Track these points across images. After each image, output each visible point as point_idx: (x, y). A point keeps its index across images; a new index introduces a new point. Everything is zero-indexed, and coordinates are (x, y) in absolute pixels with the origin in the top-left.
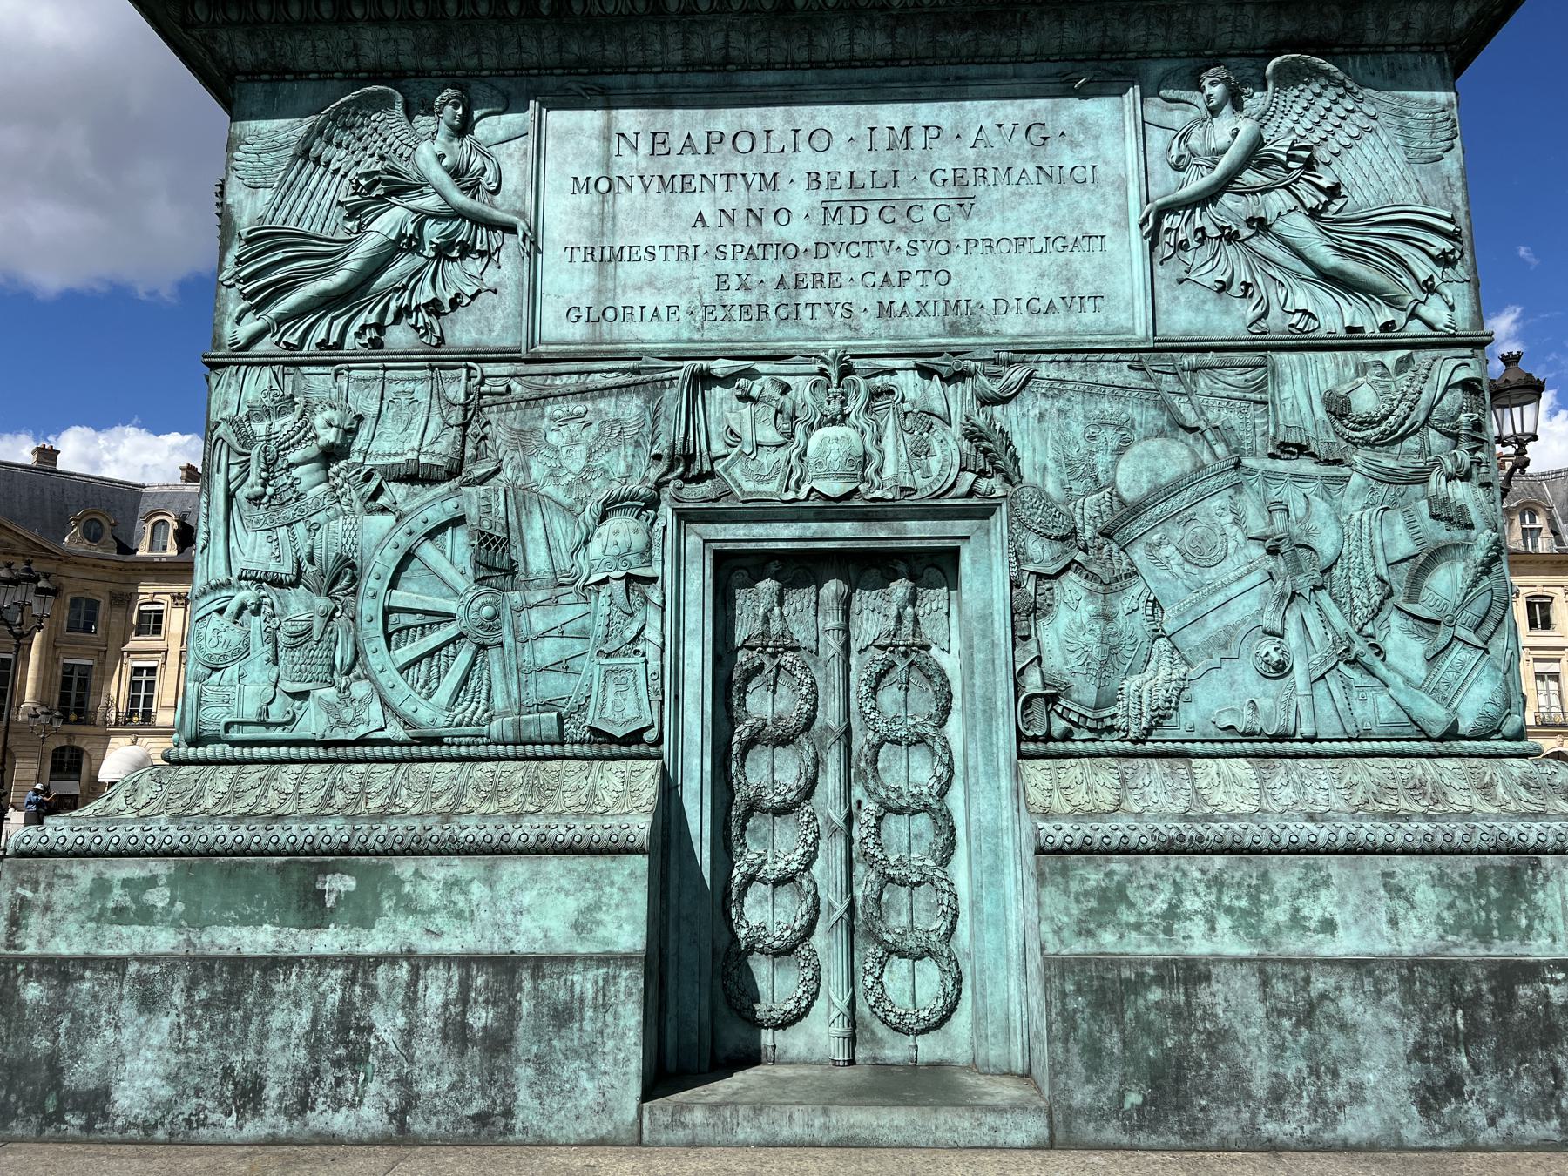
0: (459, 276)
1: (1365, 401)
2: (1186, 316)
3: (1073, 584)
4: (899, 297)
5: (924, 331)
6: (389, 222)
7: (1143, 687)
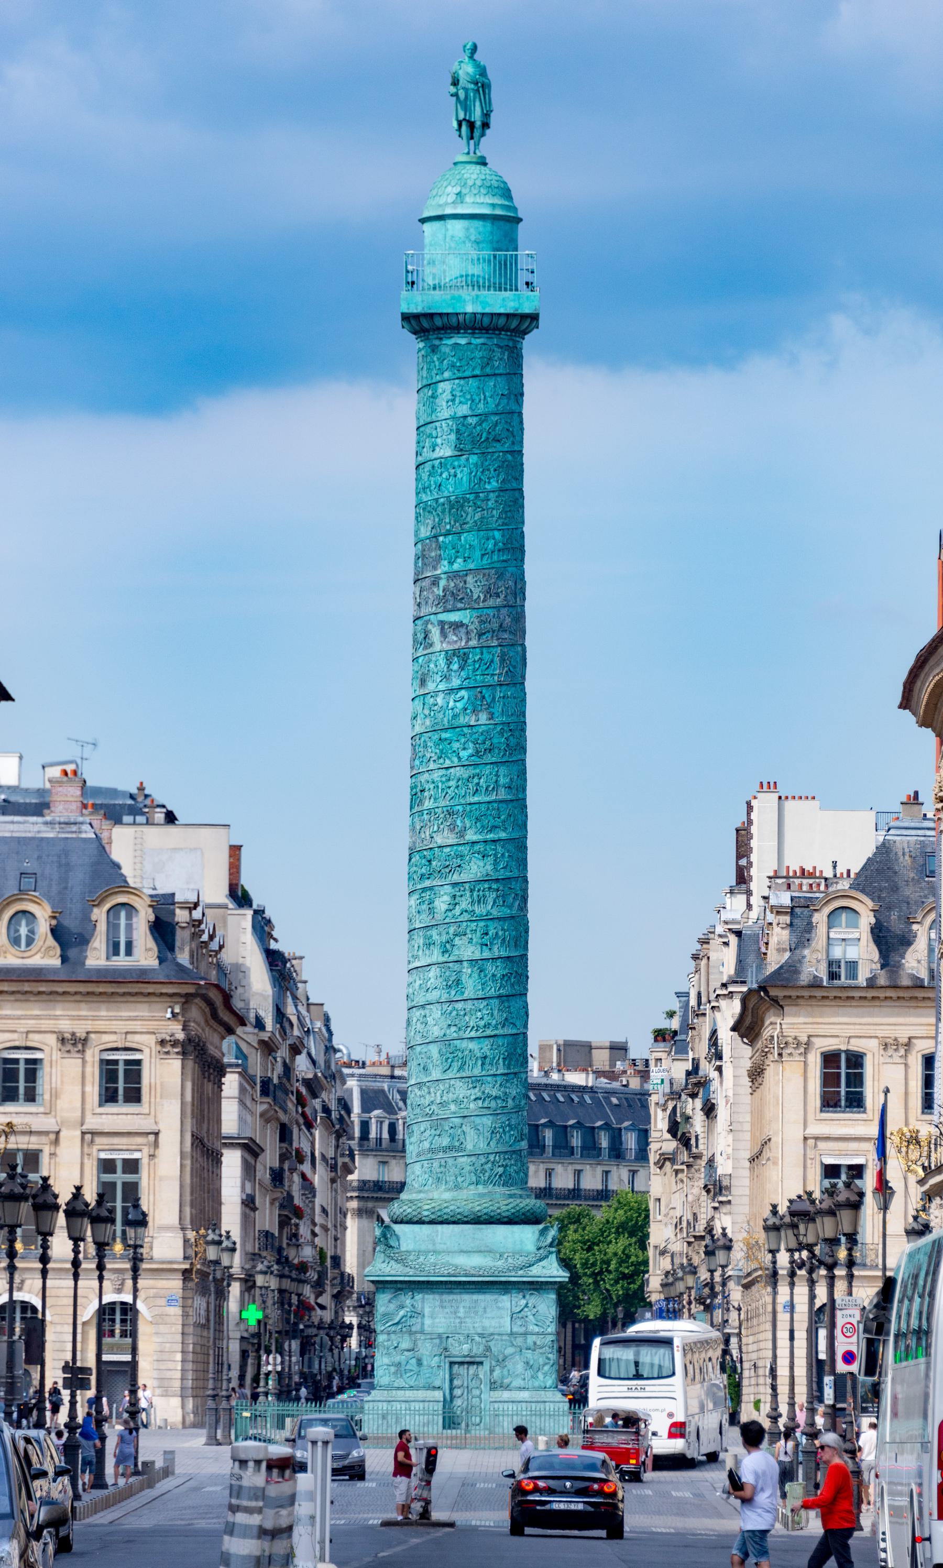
0: (413, 1321)
1: (538, 1343)
2: (515, 1329)
3: (498, 1368)
4: (476, 1325)
5: (479, 1331)
6: (402, 1313)
7: (506, 1381)
